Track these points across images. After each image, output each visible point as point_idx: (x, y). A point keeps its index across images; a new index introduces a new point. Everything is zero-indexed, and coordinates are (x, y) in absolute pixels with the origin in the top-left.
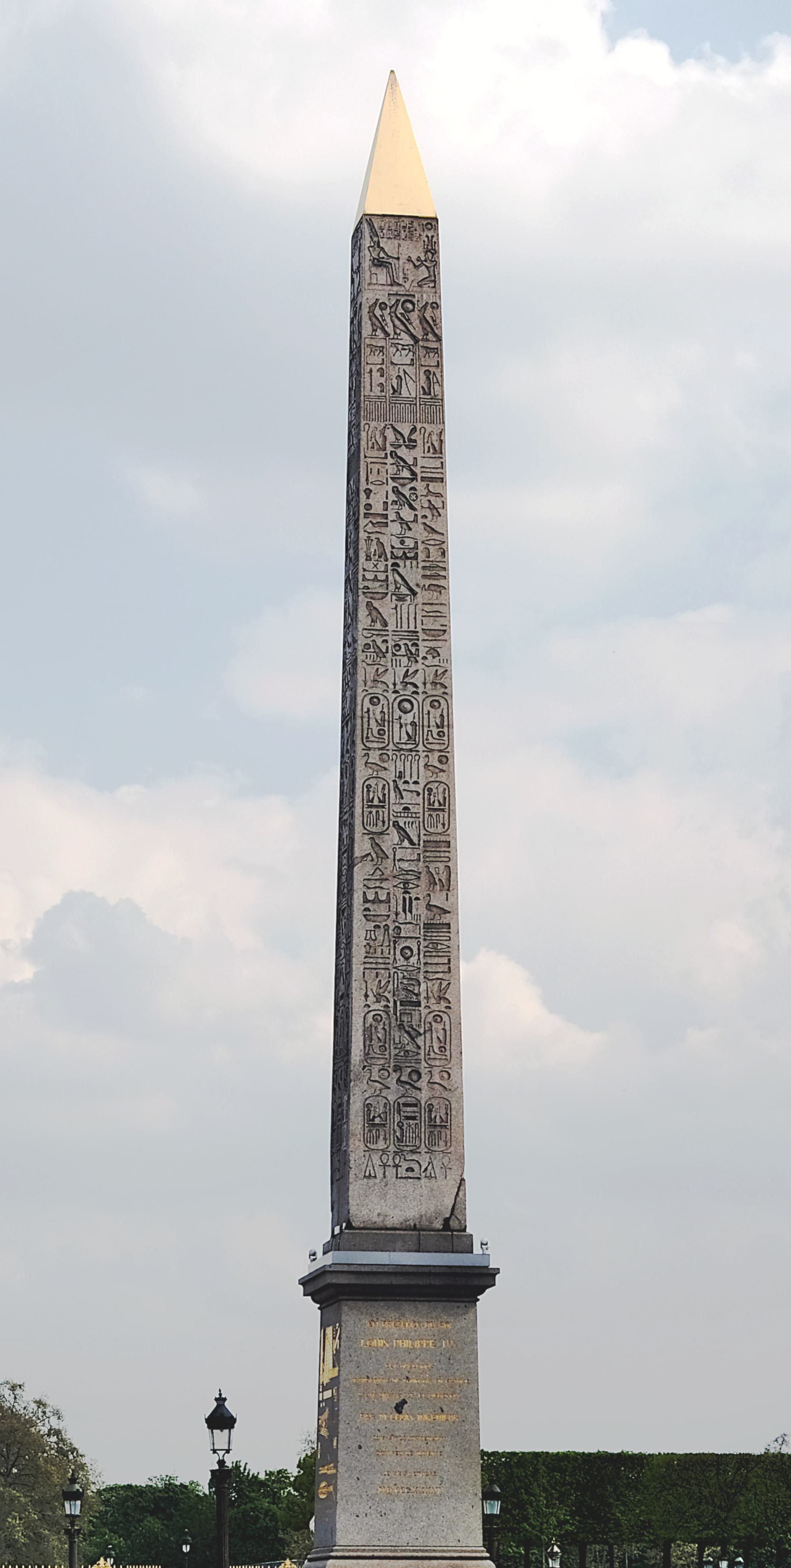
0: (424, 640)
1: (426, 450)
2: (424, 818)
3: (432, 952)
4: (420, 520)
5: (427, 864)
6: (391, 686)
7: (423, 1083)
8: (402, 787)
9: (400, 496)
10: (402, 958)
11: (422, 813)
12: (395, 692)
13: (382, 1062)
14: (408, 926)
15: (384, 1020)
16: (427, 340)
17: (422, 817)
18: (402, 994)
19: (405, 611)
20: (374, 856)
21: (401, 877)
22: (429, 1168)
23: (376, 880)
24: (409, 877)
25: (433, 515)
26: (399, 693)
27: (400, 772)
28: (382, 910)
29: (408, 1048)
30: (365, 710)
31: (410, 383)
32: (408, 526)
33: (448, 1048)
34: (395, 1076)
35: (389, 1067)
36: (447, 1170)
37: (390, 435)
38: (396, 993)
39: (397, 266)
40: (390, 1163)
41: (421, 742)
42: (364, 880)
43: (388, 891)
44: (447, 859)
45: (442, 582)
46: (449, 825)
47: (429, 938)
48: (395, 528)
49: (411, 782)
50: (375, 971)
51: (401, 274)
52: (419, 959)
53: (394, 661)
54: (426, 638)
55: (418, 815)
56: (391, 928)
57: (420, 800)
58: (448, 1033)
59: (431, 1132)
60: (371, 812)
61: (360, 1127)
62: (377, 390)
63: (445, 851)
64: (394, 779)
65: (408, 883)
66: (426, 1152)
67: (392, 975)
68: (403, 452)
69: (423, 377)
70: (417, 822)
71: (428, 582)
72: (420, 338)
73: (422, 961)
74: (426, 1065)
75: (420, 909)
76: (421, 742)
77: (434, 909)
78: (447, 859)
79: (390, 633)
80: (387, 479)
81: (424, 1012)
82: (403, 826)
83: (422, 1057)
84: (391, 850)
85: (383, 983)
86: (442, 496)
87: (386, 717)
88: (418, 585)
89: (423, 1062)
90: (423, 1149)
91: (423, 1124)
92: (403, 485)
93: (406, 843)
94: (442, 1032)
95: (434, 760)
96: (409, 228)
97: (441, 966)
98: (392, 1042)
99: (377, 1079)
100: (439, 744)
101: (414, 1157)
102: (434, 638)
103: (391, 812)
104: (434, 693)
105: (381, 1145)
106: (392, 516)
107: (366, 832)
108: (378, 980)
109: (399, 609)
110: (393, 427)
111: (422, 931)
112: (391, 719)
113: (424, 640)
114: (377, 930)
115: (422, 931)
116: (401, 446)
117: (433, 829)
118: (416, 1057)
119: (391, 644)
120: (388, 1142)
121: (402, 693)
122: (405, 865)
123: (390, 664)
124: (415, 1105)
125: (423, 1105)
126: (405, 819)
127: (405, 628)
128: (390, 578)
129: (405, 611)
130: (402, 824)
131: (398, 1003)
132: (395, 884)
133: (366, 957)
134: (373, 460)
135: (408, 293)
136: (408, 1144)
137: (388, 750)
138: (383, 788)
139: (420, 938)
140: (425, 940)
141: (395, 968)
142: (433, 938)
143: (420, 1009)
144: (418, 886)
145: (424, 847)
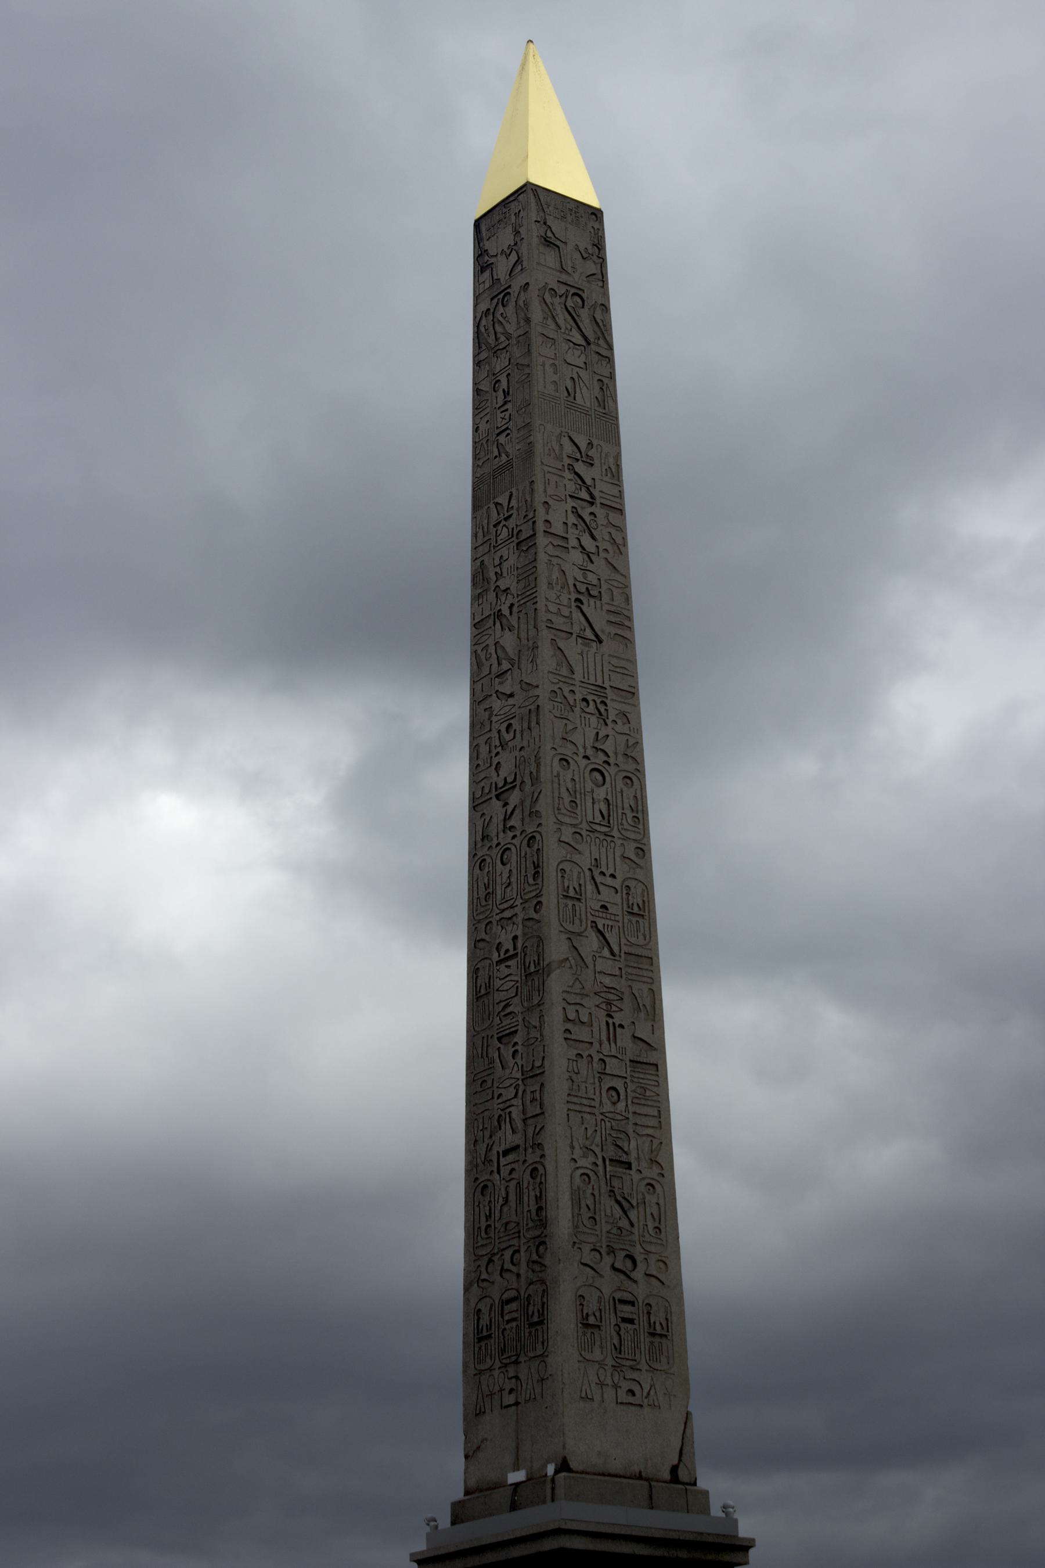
0: (612, 700)
1: (604, 473)
2: (623, 923)
3: (640, 1098)
4: (603, 554)
5: (629, 983)
6: (581, 750)
7: (638, 1274)
8: (599, 879)
9: (580, 520)
10: (609, 1103)
11: (621, 916)
12: (586, 757)
13: (592, 1239)
14: (614, 1060)
15: (592, 1183)
16: (598, 345)
17: (621, 921)
18: (611, 1152)
19: (591, 660)
20: (573, 962)
21: (603, 995)
22: (652, 1392)
23: (575, 993)
24: (611, 997)
25: (614, 552)
26: (589, 759)
27: (596, 859)
28: (582, 1033)
29: (621, 1224)
30: (555, 774)
31: (584, 390)
32: (589, 557)
33: (662, 1227)
34: (608, 1260)
35: (602, 1247)
36: (672, 1398)
37: (568, 448)
38: (604, 1147)
39: (565, 251)
40: (609, 1381)
41: (616, 827)
42: (564, 992)
43: (589, 1011)
44: (650, 981)
45: (626, 634)
46: (650, 937)
47: (636, 1080)
48: (577, 557)
49: (608, 874)
50: (580, 1115)
51: (569, 262)
52: (627, 1105)
53: (583, 719)
54: (615, 698)
55: (617, 918)
56: (596, 1059)
57: (617, 899)
58: (662, 1209)
59: (652, 1343)
60: (567, 906)
61: (572, 1326)
62: (550, 388)
63: (647, 970)
64: (589, 867)
65: (610, 1004)
66: (646, 1370)
67: (599, 1123)
68: (580, 468)
69: (597, 386)
70: (617, 928)
71: (613, 630)
72: (592, 340)
73: (631, 1109)
74: (642, 1251)
75: (624, 1037)
76: (616, 827)
77: (640, 1043)
78: (650, 981)
79: (578, 683)
80: (566, 495)
81: (636, 1177)
82: (602, 929)
83: (636, 1238)
84: (590, 959)
85: (590, 1132)
86: (622, 531)
87: (577, 786)
88: (603, 631)
89: (638, 1246)
90: (644, 1366)
91: (642, 1330)
92: (583, 508)
93: (606, 952)
94: (655, 1207)
95: (631, 854)
96: (575, 212)
97: (651, 1118)
98: (603, 1214)
99: (589, 1262)
100: (634, 832)
101: (635, 1375)
102: (622, 700)
103: (589, 910)
104: (626, 767)
105: (597, 1355)
106: (573, 542)
107: (562, 929)
108: (583, 1127)
109: (585, 656)
110: (570, 437)
111: (629, 1070)
112: (583, 791)
113: (612, 700)
114: (580, 1060)
115: (629, 1070)
116: (578, 460)
117: (633, 939)
118: (630, 1238)
119: (579, 696)
120: (604, 1353)
121: (593, 760)
122: (607, 981)
123: (579, 721)
124: (632, 1304)
125: (641, 1304)
126: (603, 921)
127: (592, 680)
128: (574, 615)
129: (591, 660)
130: (600, 927)
131: (607, 1162)
132: (597, 1003)
133: (569, 1095)
134: (550, 469)
135: (577, 286)
136: (627, 1356)
137: (582, 829)
138: (579, 878)
139: (626, 1078)
140: (632, 1081)
141: (602, 1114)
142: (641, 1081)
143: (632, 1172)
144: (622, 1010)
145: (625, 960)
